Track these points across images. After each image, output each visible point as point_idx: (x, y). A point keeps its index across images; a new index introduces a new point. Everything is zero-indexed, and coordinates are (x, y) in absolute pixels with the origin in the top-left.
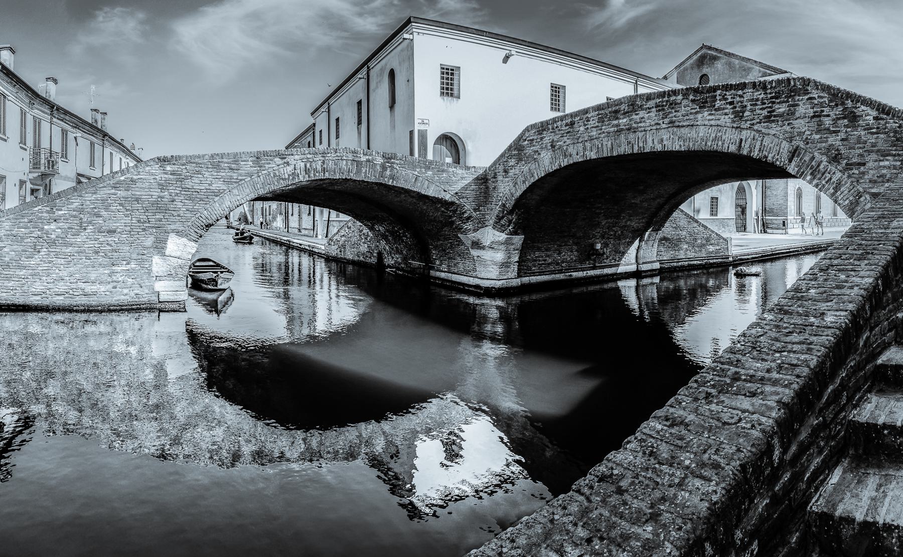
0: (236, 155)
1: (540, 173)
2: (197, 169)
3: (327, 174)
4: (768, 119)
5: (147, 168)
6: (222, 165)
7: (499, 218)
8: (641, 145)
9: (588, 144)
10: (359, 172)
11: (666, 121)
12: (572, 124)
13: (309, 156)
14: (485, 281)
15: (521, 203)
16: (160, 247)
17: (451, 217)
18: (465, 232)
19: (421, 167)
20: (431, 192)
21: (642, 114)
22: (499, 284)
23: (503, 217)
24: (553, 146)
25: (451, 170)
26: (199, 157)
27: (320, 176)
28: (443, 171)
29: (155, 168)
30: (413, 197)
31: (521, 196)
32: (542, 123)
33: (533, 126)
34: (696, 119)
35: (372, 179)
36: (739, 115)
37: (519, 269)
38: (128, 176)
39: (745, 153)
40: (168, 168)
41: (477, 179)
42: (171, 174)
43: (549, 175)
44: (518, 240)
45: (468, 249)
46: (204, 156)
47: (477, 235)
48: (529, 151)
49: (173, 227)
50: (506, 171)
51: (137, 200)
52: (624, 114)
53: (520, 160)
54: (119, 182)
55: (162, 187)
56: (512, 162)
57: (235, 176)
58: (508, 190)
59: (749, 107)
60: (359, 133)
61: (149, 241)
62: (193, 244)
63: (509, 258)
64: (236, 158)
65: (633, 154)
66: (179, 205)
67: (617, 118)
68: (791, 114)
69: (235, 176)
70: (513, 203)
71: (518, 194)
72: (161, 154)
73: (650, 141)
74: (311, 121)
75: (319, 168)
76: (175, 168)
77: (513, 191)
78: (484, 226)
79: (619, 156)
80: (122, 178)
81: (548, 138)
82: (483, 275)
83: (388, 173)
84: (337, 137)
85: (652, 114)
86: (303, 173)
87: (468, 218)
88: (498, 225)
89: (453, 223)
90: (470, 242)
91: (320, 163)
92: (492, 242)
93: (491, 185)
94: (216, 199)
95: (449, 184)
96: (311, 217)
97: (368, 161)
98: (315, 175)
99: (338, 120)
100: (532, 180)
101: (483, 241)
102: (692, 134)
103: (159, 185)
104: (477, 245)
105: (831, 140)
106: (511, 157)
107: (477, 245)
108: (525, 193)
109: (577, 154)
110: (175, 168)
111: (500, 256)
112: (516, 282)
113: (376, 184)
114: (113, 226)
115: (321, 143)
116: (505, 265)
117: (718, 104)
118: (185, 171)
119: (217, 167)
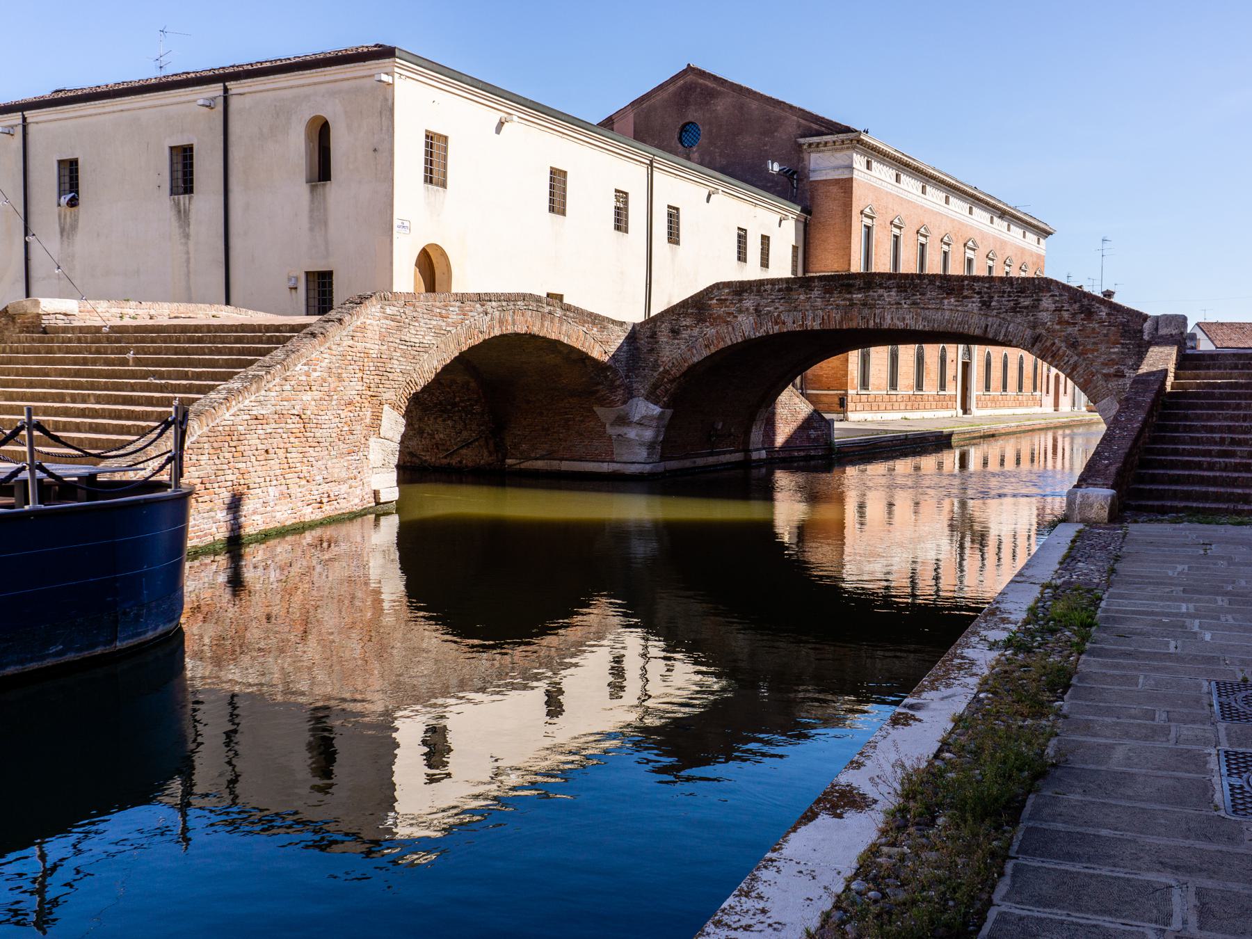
1: (732, 337)
4: (1015, 309)
7: (655, 387)
8: (878, 321)
9: (810, 315)
11: (908, 302)
12: (789, 289)
17: (598, 384)
18: (612, 404)
20: (596, 353)
21: (881, 291)
22: (648, 468)
31: (699, 363)
32: (741, 283)
34: (942, 303)
36: (986, 305)
39: (990, 336)
44: (669, 412)
45: (604, 426)
50: (675, 332)
52: (860, 289)
56: (688, 322)
58: (674, 353)
59: (996, 298)
63: (657, 436)
65: (867, 330)
67: (850, 293)
68: (1035, 307)
71: (695, 360)
73: (888, 318)
78: (632, 397)
79: (848, 330)
81: (749, 303)
82: (625, 459)
85: (893, 293)
87: (619, 386)
88: (652, 397)
90: (612, 417)
92: (643, 417)
93: (643, 342)
100: (722, 345)
102: (938, 315)
104: (623, 420)
105: (1070, 330)
106: (686, 315)
107: (623, 420)
109: (791, 323)
111: (648, 434)
112: (661, 467)
116: (651, 446)
117: (966, 293)
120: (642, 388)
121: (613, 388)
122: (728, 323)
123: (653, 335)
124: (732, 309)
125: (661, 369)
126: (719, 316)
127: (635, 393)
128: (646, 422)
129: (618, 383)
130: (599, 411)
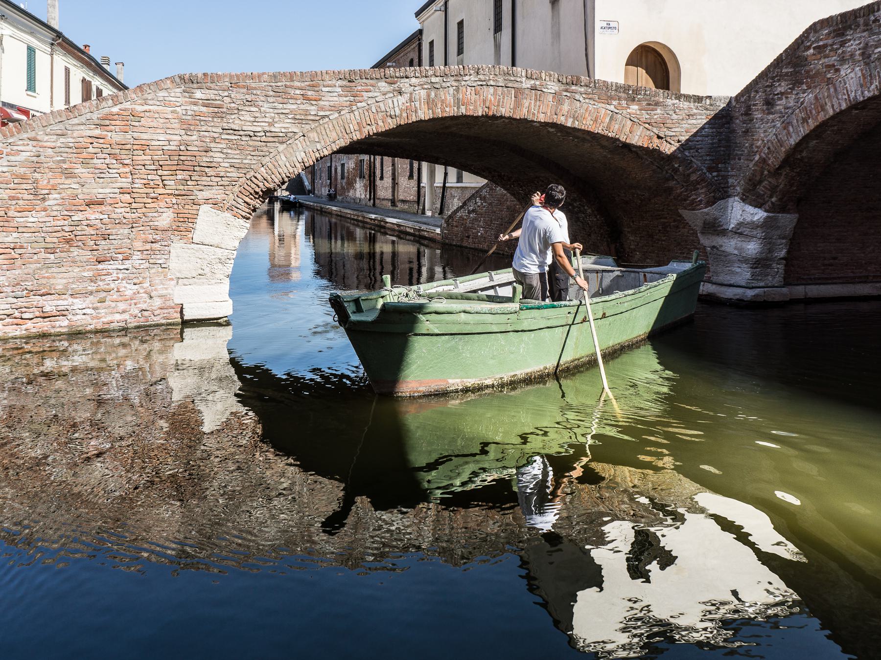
0: (313, 76)
2: (249, 98)
3: (463, 110)
5: (161, 94)
6: (292, 92)
10: (518, 104)
13: (434, 80)
14: (723, 289)
15: (792, 158)
16: (184, 225)
17: (667, 180)
18: (693, 206)
19: (619, 99)
20: (638, 138)
23: (760, 182)
24: (866, 55)
25: (669, 102)
26: (252, 77)
27: (451, 111)
28: (657, 104)
29: (176, 94)
30: (603, 147)
31: (798, 144)
32: (844, 16)
33: (823, 23)
35: (542, 118)
37: (786, 271)
38: (127, 105)
40: (198, 94)
41: (716, 117)
42: (204, 105)
43: (856, 106)
46: (260, 76)
47: (711, 211)
48: (818, 64)
49: (206, 194)
51: (145, 147)
53: (796, 82)
54: (109, 117)
55: (187, 127)
56: (782, 87)
57: (313, 110)
58: (773, 135)
60: (497, 47)
61: (166, 219)
62: (242, 221)
64: (314, 80)
66: (218, 157)
69: (313, 110)
70: (782, 156)
72: (186, 71)
74: (415, 26)
75: (450, 99)
76: (211, 94)
77: (783, 136)
80: (115, 110)
83: (566, 107)
84: (460, 51)
86: (425, 107)
88: (752, 197)
89: (670, 190)
91: (451, 90)
93: (738, 124)
94: (281, 147)
95: (666, 127)
96: (413, 183)
97: (534, 88)
98: (443, 111)
99: (461, 24)
100: (822, 117)
101: (722, 220)
103: (182, 122)
108: (806, 138)
110: (211, 94)
113: (546, 124)
114: (97, 190)
115: (431, 64)
118: (227, 100)
119: (281, 94)
120: (737, 184)
121: (694, 186)
122: (829, 81)
123: (748, 112)
124: (833, 59)
125: (757, 158)
126: (818, 73)
127: (731, 191)
128: (747, 231)
129: (693, 177)
130: (685, 214)
